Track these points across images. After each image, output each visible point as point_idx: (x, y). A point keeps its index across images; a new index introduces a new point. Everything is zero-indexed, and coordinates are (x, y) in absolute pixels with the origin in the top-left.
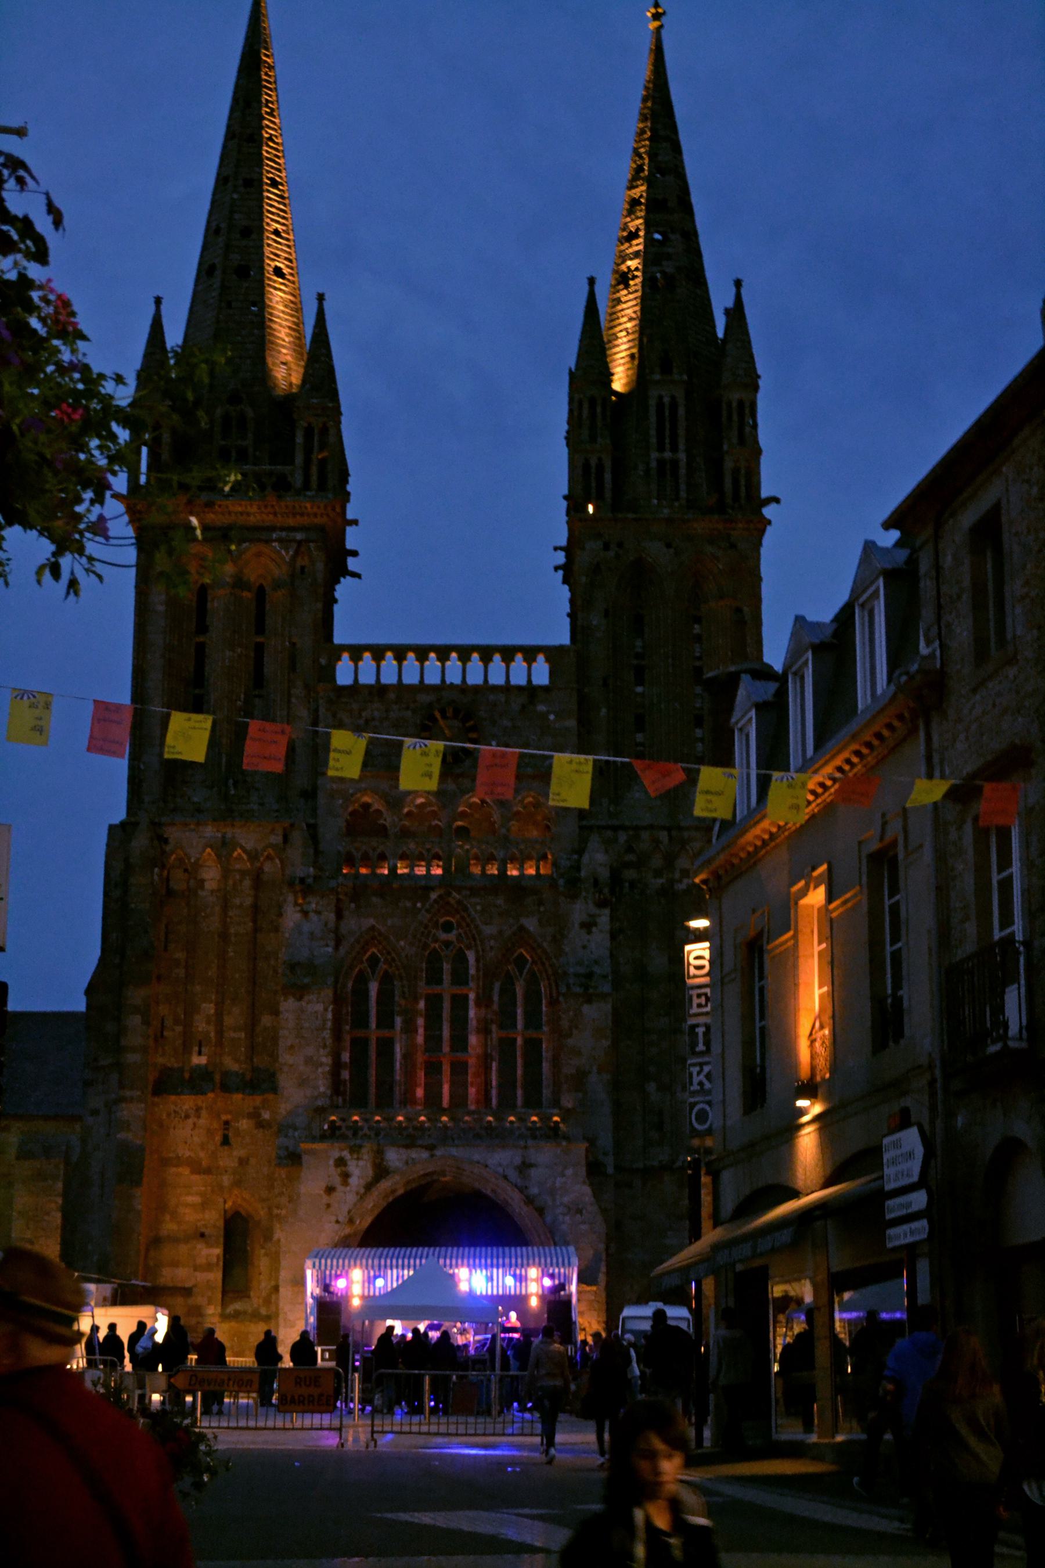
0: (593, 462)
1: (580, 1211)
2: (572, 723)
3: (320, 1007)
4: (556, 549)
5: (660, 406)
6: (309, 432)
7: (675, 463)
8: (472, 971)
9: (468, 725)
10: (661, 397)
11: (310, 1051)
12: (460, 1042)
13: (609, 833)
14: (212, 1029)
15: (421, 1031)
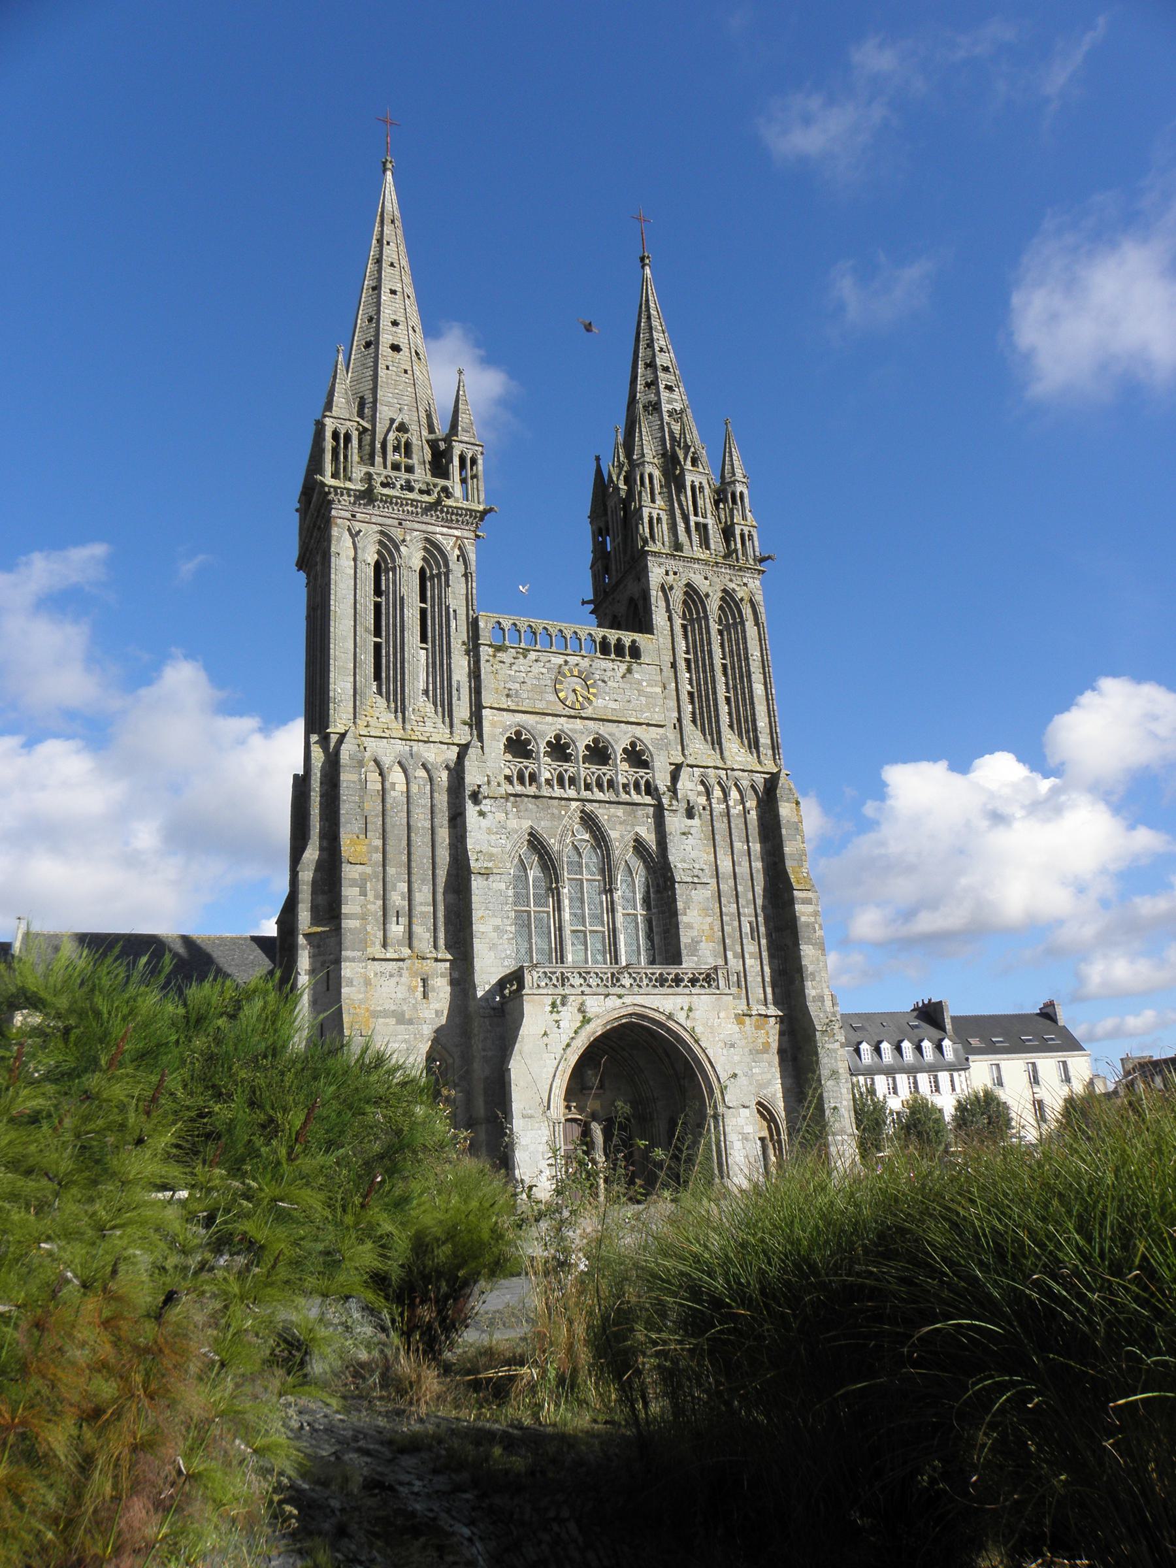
0: (655, 516)
1: (732, 1046)
2: (659, 690)
3: (503, 886)
5: (693, 488)
6: (462, 459)
7: (705, 526)
10: (693, 482)
11: (498, 921)
14: (406, 903)
15: (567, 909)
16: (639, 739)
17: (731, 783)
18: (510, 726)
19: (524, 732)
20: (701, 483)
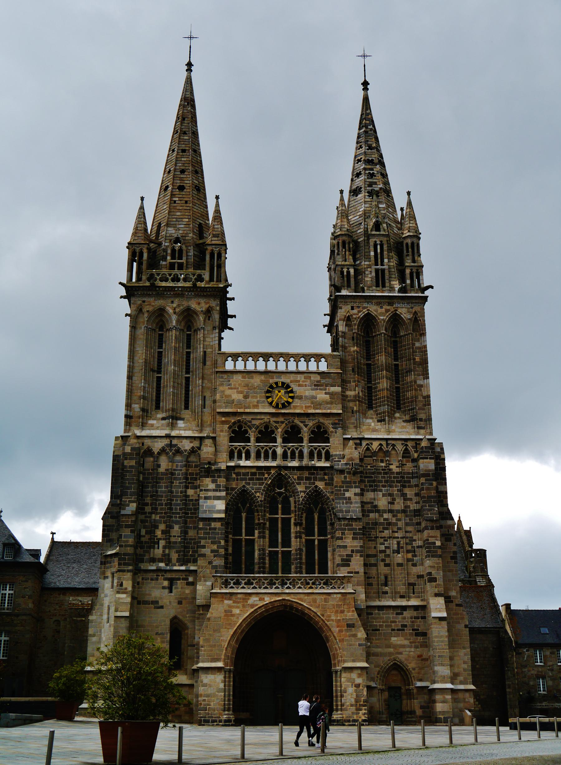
4: (325, 315)
8: (292, 508)
9: (289, 390)
12: (287, 543)
13: (358, 441)
16: (324, 424)
17: (390, 448)
18: (234, 423)
19: (244, 425)
20: (381, 241)
